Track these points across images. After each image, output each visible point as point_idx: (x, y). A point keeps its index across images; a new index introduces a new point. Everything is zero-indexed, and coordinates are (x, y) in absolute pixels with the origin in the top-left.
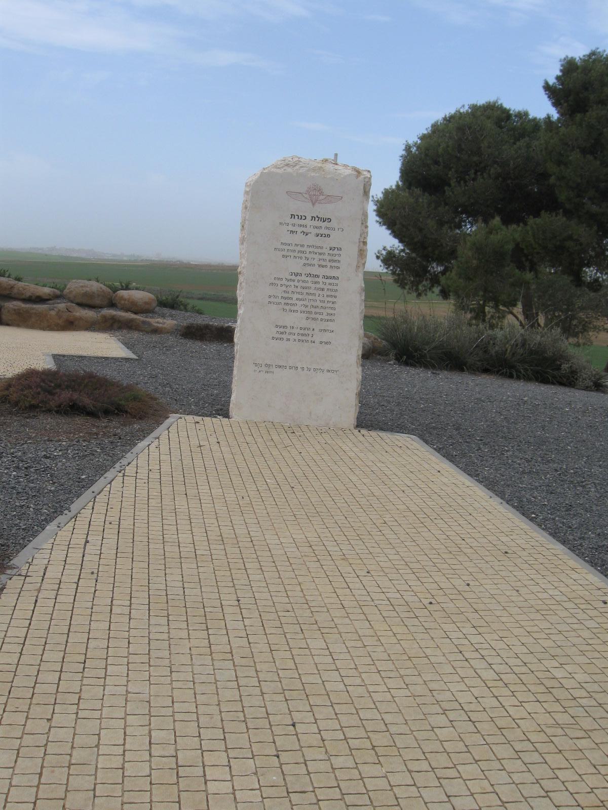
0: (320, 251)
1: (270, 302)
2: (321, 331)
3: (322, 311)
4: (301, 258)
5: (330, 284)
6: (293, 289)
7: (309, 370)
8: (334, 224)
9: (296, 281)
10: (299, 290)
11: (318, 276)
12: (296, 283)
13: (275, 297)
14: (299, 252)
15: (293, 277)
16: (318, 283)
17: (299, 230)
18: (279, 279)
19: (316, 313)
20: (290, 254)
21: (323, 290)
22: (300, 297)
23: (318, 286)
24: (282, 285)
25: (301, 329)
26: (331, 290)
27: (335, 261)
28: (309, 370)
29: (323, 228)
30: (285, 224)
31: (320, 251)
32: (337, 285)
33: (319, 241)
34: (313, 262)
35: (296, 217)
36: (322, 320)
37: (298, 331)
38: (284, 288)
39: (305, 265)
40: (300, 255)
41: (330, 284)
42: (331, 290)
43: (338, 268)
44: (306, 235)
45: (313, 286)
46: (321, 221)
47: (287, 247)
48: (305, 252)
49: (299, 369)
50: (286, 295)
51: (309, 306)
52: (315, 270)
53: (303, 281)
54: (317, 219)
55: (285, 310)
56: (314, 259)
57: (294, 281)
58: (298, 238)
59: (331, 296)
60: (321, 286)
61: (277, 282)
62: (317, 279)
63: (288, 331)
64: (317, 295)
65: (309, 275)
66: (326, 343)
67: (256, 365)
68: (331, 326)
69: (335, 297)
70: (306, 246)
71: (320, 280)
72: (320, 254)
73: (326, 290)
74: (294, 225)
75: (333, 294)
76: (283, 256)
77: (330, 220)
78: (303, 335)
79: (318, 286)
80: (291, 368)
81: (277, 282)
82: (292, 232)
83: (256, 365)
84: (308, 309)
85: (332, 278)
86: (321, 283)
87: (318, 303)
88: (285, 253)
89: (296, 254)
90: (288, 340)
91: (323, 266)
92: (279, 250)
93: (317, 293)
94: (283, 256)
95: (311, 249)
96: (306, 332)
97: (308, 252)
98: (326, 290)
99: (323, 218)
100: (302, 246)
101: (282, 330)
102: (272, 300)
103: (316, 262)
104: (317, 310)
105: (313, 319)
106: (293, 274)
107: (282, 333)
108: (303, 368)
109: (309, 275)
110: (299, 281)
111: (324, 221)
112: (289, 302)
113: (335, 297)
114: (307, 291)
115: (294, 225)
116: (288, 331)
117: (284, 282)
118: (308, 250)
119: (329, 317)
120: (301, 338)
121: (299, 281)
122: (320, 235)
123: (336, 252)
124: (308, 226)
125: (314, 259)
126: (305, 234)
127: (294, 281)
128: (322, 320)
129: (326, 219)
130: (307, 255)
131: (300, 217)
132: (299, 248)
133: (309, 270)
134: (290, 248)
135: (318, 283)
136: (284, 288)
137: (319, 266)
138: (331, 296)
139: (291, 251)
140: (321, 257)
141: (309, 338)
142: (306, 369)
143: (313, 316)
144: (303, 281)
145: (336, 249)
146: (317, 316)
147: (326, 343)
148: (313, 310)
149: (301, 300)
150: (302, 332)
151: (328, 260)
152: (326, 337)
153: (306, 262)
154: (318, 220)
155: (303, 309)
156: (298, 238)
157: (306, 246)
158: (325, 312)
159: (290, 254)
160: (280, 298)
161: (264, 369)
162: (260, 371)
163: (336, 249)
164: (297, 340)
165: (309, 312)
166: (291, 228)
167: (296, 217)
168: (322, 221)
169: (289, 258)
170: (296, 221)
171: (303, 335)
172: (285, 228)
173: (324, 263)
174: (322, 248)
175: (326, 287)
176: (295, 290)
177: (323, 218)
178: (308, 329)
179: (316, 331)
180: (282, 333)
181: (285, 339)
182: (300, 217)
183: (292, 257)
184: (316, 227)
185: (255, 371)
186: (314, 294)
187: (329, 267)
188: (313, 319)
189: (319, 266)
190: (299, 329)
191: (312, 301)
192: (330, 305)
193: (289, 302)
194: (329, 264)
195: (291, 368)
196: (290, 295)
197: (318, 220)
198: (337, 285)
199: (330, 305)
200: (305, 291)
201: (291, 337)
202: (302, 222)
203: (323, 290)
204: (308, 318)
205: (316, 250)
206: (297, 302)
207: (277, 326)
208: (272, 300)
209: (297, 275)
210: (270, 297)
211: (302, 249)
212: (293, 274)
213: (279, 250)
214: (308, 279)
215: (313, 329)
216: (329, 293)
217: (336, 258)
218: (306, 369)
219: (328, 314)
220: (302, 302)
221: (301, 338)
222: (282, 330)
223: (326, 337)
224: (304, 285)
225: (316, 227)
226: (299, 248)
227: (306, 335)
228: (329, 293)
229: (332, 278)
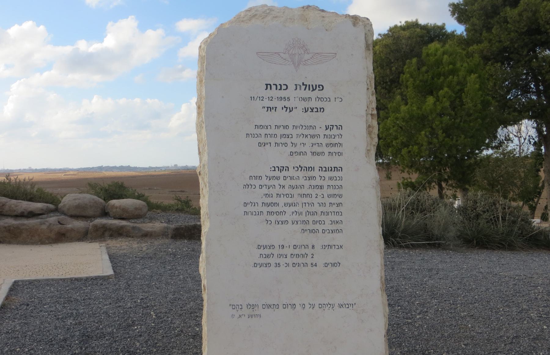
0: (311, 132)
1: (246, 213)
2: (324, 247)
3: (323, 218)
4: (285, 144)
5: (331, 178)
6: (278, 190)
7: (313, 306)
8: (327, 92)
9: (282, 178)
10: (287, 191)
11: (313, 169)
12: (282, 182)
13: (254, 204)
14: (281, 136)
15: (277, 173)
16: (314, 178)
17: (280, 105)
18: (256, 177)
19: (315, 222)
20: (269, 140)
21: (321, 187)
22: (290, 200)
23: (313, 183)
24: (261, 186)
25: (295, 247)
26: (334, 187)
27: (335, 145)
28: (313, 306)
29: (313, 99)
30: (258, 99)
31: (311, 132)
32: (341, 178)
33: (310, 119)
34: (303, 149)
35: (274, 87)
36: (324, 231)
37: (291, 251)
38: (265, 190)
39: (292, 154)
40: (283, 140)
41: (331, 178)
42: (334, 187)
43: (340, 154)
44: (290, 111)
45: (307, 183)
47: (263, 132)
48: (290, 136)
49: (298, 307)
50: (268, 200)
51: (304, 214)
52: (308, 161)
53: (292, 178)
55: (269, 222)
56: (304, 144)
57: (278, 178)
58: (280, 117)
59: (334, 195)
60: (318, 182)
61: (253, 182)
62: (311, 174)
63: (276, 252)
64: (314, 196)
66: (333, 265)
67: (233, 306)
68: (338, 239)
69: (340, 196)
70: (291, 127)
71: (316, 173)
72: (312, 136)
73: (326, 187)
74: (271, 99)
75: (336, 192)
76: (260, 144)
78: (298, 256)
79: (313, 183)
80: (285, 306)
81: (253, 182)
82: (269, 109)
83: (233, 306)
84: (303, 218)
85: (333, 169)
86: (318, 178)
87: (317, 208)
88: (262, 140)
89: (278, 140)
90: (278, 265)
91: (318, 154)
92: (253, 136)
93: (313, 192)
94: (260, 144)
95: (299, 131)
96: (303, 251)
97: (295, 136)
98: (326, 187)
100: (286, 127)
101: (267, 251)
102: (249, 208)
103: (307, 149)
104: (316, 218)
105: (311, 231)
106: (277, 169)
107: (267, 256)
108: (303, 306)
109: (300, 169)
110: (285, 178)
112: (274, 209)
113: (340, 196)
114: (299, 191)
115: (271, 99)
116: (276, 252)
117: (264, 181)
118: (295, 132)
119: (334, 227)
120: (295, 260)
121: (285, 178)
122: (310, 110)
123: (335, 131)
124: (292, 99)
125: (304, 144)
126: (288, 110)
127: (278, 178)
128: (324, 231)
129: (316, 86)
130: (294, 140)
131: (279, 87)
132: (282, 131)
133: (299, 161)
134: (268, 131)
135: (314, 178)
136: (265, 190)
137: (313, 153)
138: (334, 195)
139: (271, 136)
140: (315, 141)
141: (309, 260)
142: (307, 306)
143: (311, 227)
144: (292, 178)
145: (335, 127)
146: (317, 226)
147: (333, 265)
148: (311, 218)
149: (290, 205)
150: (297, 251)
151: (324, 145)
152: (332, 256)
153: (294, 149)
154: (305, 89)
155: (295, 217)
156: (280, 117)
157: (291, 127)
158: (327, 219)
159: (269, 140)
160: (260, 204)
161: (246, 311)
162: (240, 316)
163: (335, 127)
164: (291, 265)
165: (306, 222)
166: (267, 103)
167: (274, 87)
169: (267, 146)
170: (274, 93)
171: (298, 256)
172: (259, 104)
173: (319, 150)
174: (314, 127)
175: (325, 183)
176: (281, 191)
177: (312, 86)
178: (306, 247)
179: (318, 247)
180: (267, 256)
181: (273, 265)
182: (279, 87)
183: (273, 144)
184: (304, 99)
185: (233, 316)
186: (310, 196)
187: (327, 154)
188: (311, 231)
189: (313, 153)
190: (292, 247)
191: (307, 205)
192: (334, 208)
193: (274, 209)
194: (326, 150)
195: (285, 306)
196: (274, 200)
197: (305, 89)
198: (341, 178)
199: (334, 208)
200: (296, 192)
201: (282, 261)
202: (282, 94)
203: (321, 187)
204: (304, 231)
205: (306, 132)
206: (286, 209)
207: (259, 247)
208: (249, 208)
209: (281, 169)
210: (246, 204)
211: (286, 132)
212: (277, 169)
213: (253, 136)
214: (301, 174)
215: (313, 247)
216: (331, 191)
217: (337, 140)
218: (307, 306)
219: (332, 222)
220: (293, 209)
221: (295, 260)
222: (267, 251)
223: (332, 256)
224: (293, 183)
225: (304, 99)
226: (282, 131)
227: (303, 256)
228: (331, 191)
229: (333, 169)
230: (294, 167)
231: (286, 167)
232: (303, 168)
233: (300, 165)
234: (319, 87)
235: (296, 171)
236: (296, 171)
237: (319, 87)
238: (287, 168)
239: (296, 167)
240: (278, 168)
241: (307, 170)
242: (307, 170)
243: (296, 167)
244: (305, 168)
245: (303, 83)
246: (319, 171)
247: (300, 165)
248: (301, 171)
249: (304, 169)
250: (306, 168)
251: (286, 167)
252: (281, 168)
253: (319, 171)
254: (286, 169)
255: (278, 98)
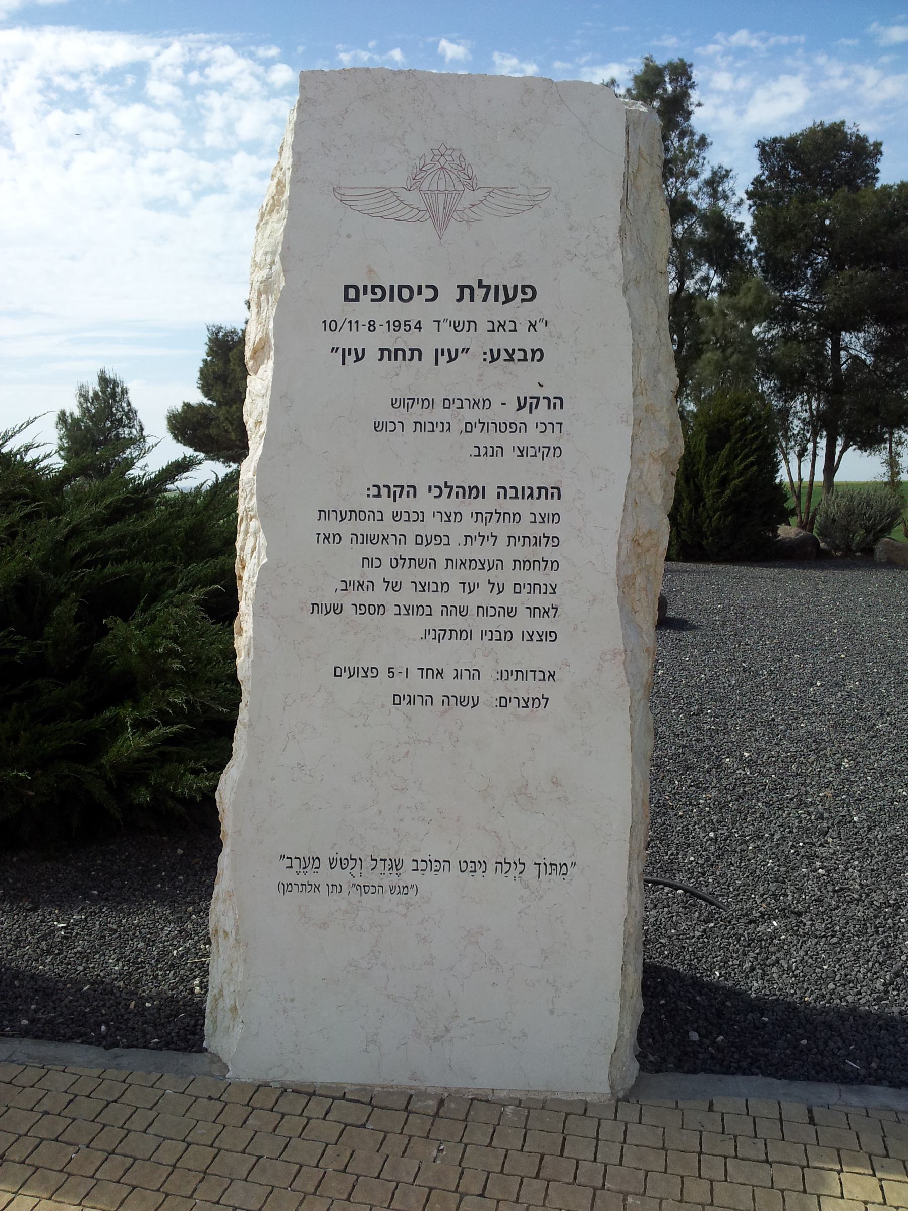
30: (347, 325)
46: (496, 300)
54: (480, 293)
65: (446, 491)
77: (529, 292)
99: (505, 287)
109: (446, 491)
111: (508, 300)
129: (515, 287)
154: (485, 300)
168: (502, 297)
177: (505, 287)
197: (485, 300)
230: (430, 487)
231: (408, 486)
232: (455, 490)
233: (446, 483)
234: (524, 293)
235: (435, 497)
236: (435, 497)
237: (524, 293)
238: (411, 490)
239: (436, 487)
240: (386, 489)
241: (464, 496)
242: (464, 496)
243: (436, 487)
244: (461, 490)
245: (480, 281)
246: (499, 498)
247: (446, 483)
248: (449, 496)
249: (457, 493)
250: (463, 488)
251: (408, 486)
252: (396, 489)
253: (499, 498)
254: (408, 492)
255: (389, 322)
